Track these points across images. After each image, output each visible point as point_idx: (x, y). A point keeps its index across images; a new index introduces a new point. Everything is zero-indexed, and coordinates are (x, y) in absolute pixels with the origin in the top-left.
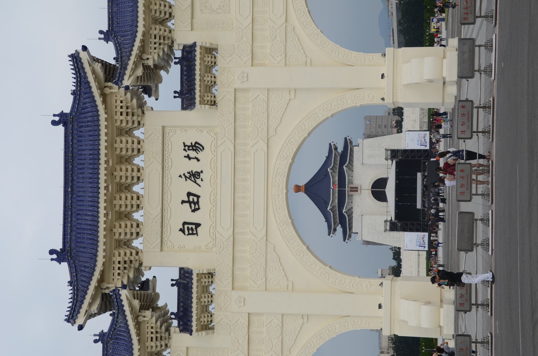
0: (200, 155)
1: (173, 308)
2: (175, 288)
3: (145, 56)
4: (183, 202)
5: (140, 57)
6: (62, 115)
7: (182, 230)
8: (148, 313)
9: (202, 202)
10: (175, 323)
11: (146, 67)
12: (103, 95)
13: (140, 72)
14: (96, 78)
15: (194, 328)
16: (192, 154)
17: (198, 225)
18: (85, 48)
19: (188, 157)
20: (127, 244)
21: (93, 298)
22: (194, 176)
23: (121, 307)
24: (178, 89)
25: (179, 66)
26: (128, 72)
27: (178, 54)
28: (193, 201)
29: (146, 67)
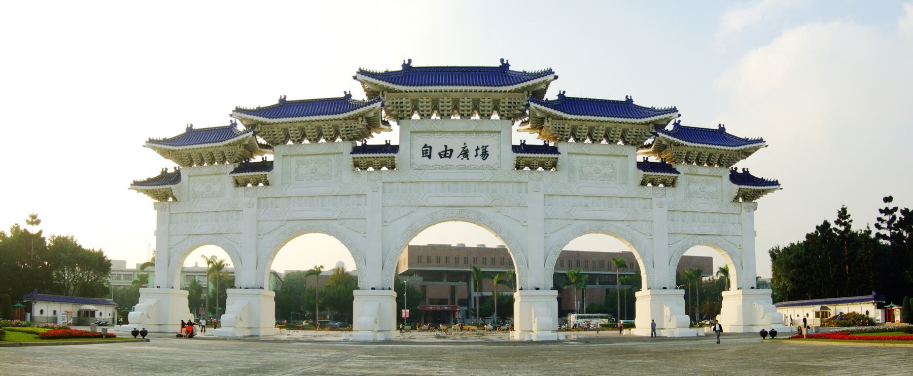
0: (479, 157)
1: (370, 142)
2: (384, 143)
3: (550, 119)
4: (446, 146)
5: (549, 115)
6: (507, 65)
7: (426, 146)
8: (365, 123)
9: (446, 160)
10: (359, 144)
11: (543, 119)
12: (523, 89)
13: (538, 115)
14: (534, 85)
15: (355, 156)
16: (480, 152)
17: (430, 157)
18: (556, 78)
19: (478, 149)
20: (415, 108)
21: (376, 85)
22: (465, 153)
23: (369, 104)
24: (527, 143)
25: (542, 144)
26: (539, 106)
27: (551, 144)
28: (446, 153)
29: (542, 120)
